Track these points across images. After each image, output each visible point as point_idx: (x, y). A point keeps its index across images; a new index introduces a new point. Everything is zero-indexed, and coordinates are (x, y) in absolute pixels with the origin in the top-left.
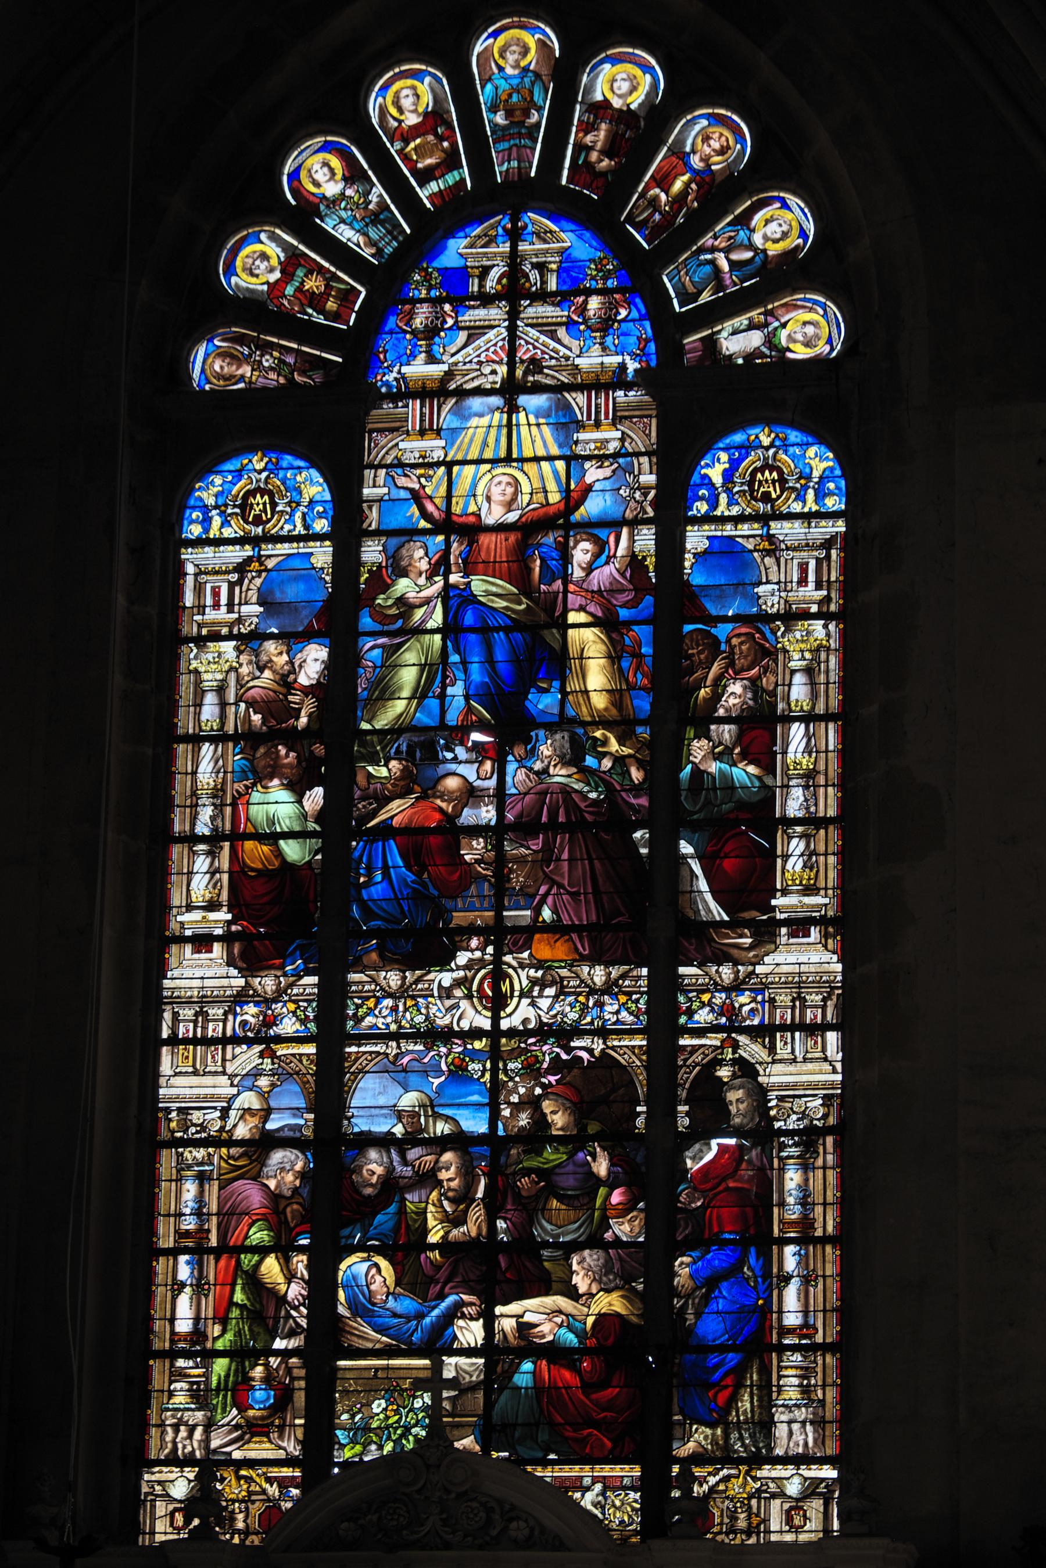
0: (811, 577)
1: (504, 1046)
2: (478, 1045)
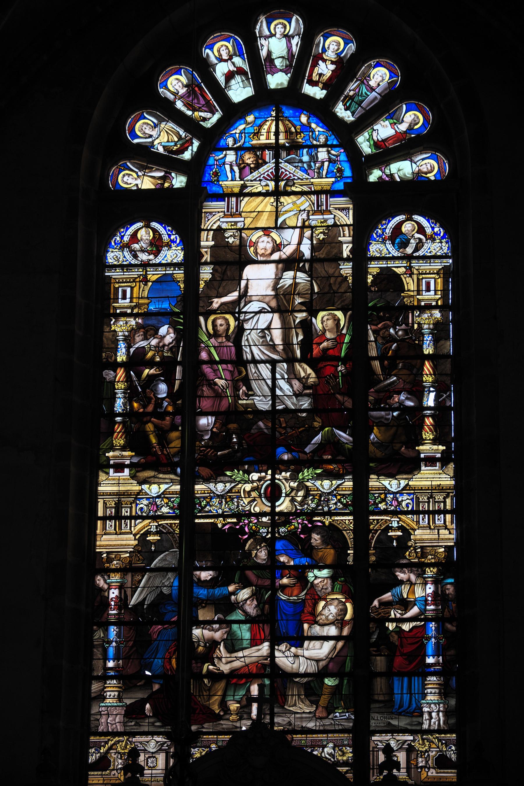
0: (432, 287)
1: (277, 520)
2: (265, 519)
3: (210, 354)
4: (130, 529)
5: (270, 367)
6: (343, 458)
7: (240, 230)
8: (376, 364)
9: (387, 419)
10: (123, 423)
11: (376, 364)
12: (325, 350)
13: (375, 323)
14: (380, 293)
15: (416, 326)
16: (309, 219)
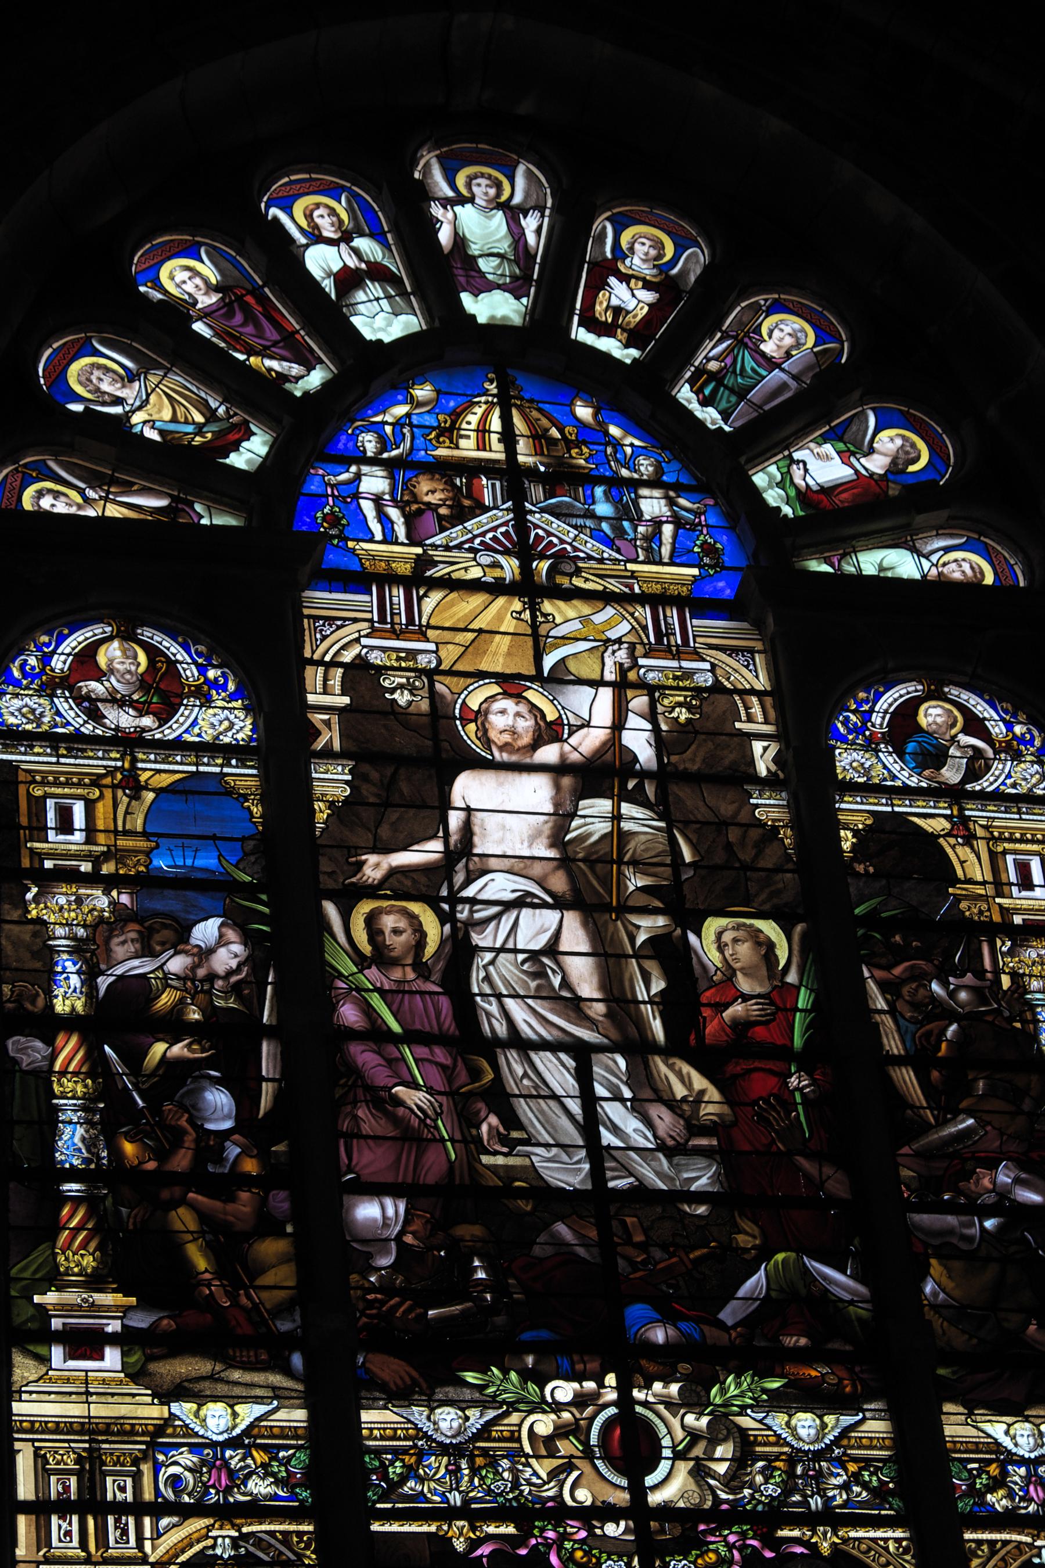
2: (612, 1529)
3: (368, 1010)
4: (140, 1546)
5: (571, 1063)
6: (848, 1348)
7: (430, 674)
8: (907, 1078)
9: (970, 1239)
10: (87, 1200)
11: (907, 1078)
12: (741, 1026)
13: (883, 961)
14: (884, 882)
15: (1006, 981)
16: (635, 665)
